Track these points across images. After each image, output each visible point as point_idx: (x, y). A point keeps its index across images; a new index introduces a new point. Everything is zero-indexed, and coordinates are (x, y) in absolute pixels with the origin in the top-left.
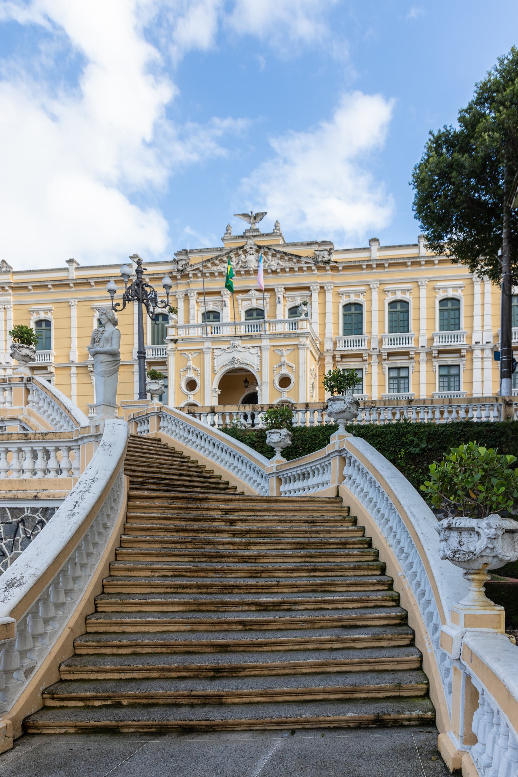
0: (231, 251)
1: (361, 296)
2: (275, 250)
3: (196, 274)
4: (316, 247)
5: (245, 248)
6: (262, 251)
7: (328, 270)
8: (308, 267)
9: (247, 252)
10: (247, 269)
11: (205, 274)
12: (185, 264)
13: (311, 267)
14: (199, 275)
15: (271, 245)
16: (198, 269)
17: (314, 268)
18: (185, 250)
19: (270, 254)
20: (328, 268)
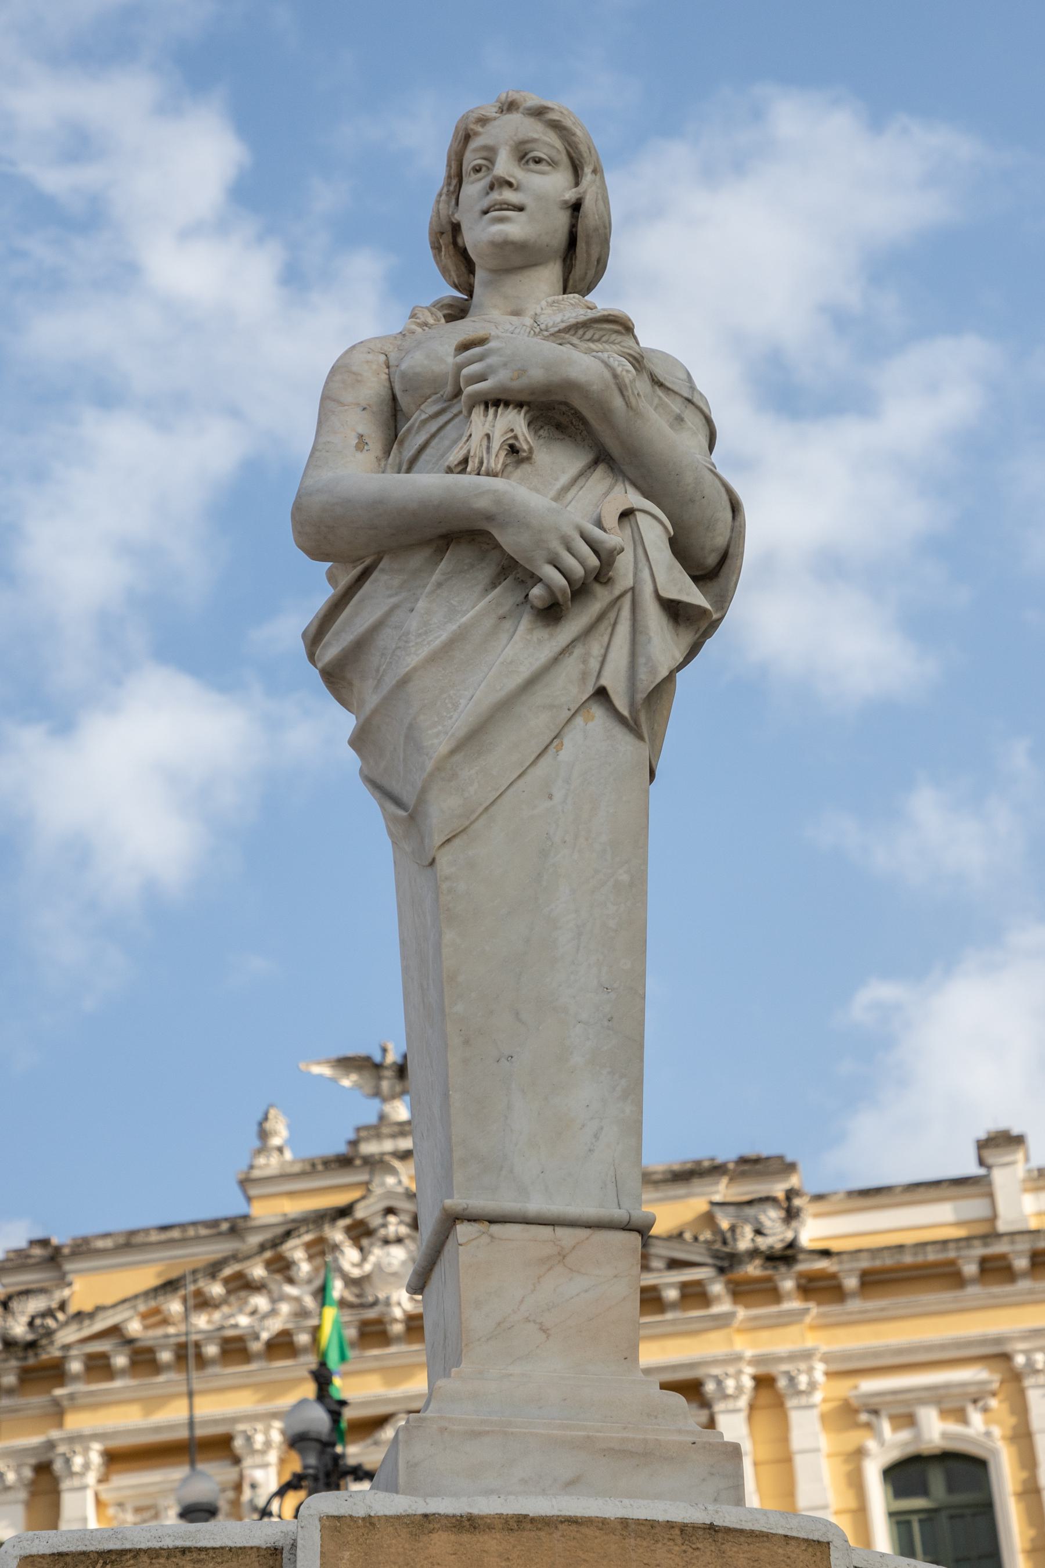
0: (288, 1235)
1: (976, 1418)
3: (104, 1356)
4: (722, 1190)
5: (360, 1213)
7: (789, 1296)
8: (684, 1286)
9: (369, 1233)
10: (371, 1314)
11: (151, 1351)
12: (49, 1313)
13: (699, 1283)
14: (120, 1361)
16: (115, 1331)
17: (717, 1288)
18: (44, 1243)
20: (788, 1285)
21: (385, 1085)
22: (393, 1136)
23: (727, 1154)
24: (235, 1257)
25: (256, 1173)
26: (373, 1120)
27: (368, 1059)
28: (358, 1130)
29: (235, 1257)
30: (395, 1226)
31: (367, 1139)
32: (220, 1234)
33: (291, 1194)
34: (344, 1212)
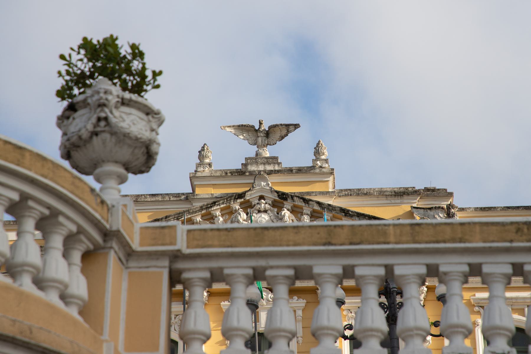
0: (214, 203)
2: (319, 203)
4: (417, 202)
6: (288, 204)
9: (252, 207)
15: (308, 193)
19: (307, 210)
21: (260, 140)
22: (264, 164)
23: (420, 186)
24: (188, 212)
25: (199, 174)
26: (253, 155)
27: (253, 127)
28: (246, 159)
29: (188, 212)
30: (263, 205)
31: (251, 164)
32: (181, 200)
33: (214, 186)
34: (241, 196)
